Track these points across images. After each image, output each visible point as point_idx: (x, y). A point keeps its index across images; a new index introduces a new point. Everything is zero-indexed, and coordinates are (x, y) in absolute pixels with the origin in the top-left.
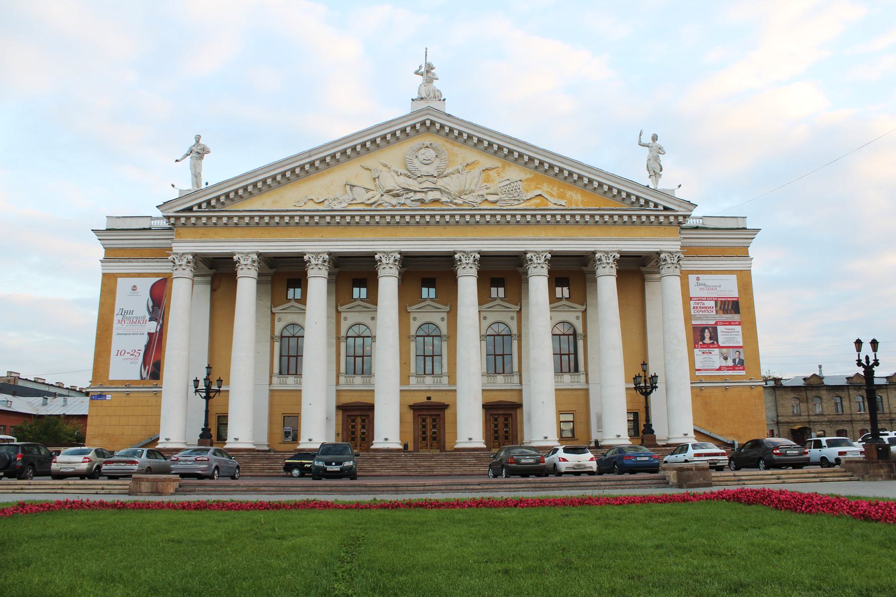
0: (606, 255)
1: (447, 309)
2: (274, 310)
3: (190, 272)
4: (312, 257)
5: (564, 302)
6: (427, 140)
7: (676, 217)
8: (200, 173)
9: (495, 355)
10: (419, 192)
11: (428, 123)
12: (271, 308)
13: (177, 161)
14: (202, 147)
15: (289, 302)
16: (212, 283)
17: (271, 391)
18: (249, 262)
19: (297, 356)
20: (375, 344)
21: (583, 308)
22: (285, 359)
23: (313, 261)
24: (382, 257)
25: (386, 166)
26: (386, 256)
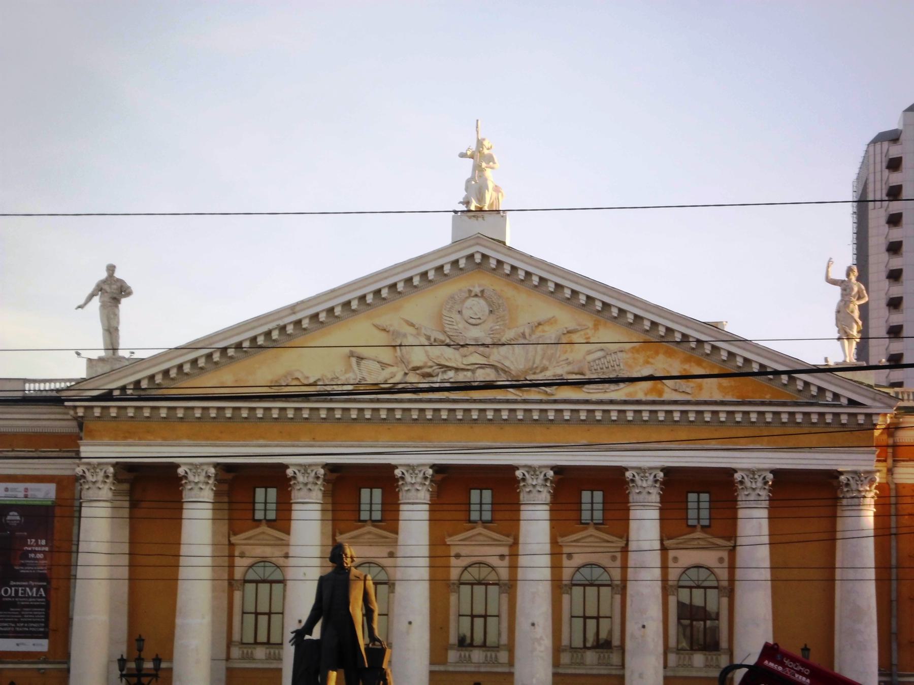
0: (752, 476)
1: (508, 541)
2: (234, 539)
3: (109, 491)
4: (299, 471)
5: (698, 534)
6: (478, 282)
7: (869, 416)
8: (117, 330)
9: (585, 618)
10: (463, 370)
11: (478, 259)
12: (229, 537)
13: (80, 307)
14: (119, 284)
15: (258, 526)
16: (131, 493)
17: (230, 671)
18: (202, 478)
19: (269, 614)
20: (394, 596)
21: (731, 543)
22: (250, 619)
23: (301, 478)
24: (405, 473)
25: (412, 325)
26: (411, 471)
